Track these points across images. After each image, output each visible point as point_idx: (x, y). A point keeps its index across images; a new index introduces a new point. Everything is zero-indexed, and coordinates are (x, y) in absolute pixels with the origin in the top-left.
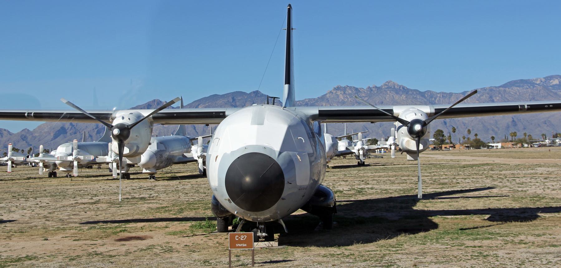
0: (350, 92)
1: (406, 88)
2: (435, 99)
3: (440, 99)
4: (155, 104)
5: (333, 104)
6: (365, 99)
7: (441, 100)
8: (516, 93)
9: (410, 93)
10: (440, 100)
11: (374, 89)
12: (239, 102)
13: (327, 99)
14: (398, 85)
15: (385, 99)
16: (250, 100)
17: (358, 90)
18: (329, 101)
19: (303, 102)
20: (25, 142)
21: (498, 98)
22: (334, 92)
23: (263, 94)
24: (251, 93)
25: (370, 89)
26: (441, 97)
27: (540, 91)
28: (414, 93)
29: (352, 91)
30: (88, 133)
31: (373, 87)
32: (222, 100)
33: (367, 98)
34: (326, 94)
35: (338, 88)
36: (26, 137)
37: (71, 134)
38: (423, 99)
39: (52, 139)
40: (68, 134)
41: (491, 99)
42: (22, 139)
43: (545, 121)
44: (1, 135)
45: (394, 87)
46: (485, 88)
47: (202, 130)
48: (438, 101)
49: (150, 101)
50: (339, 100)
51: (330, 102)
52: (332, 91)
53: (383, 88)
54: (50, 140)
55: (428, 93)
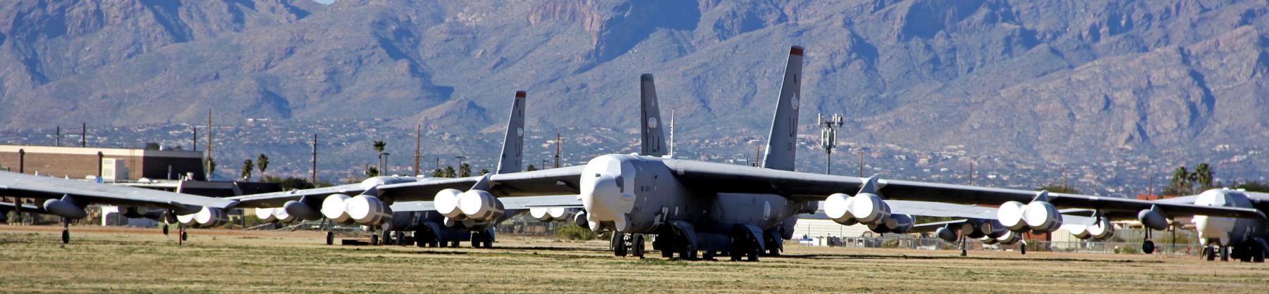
20: (403, 65)
30: (848, 23)
36: (409, 34)
37: (718, 26)
39: (588, 56)
40: (705, 27)
42: (385, 43)
44: (231, 10)
54: (578, 61)
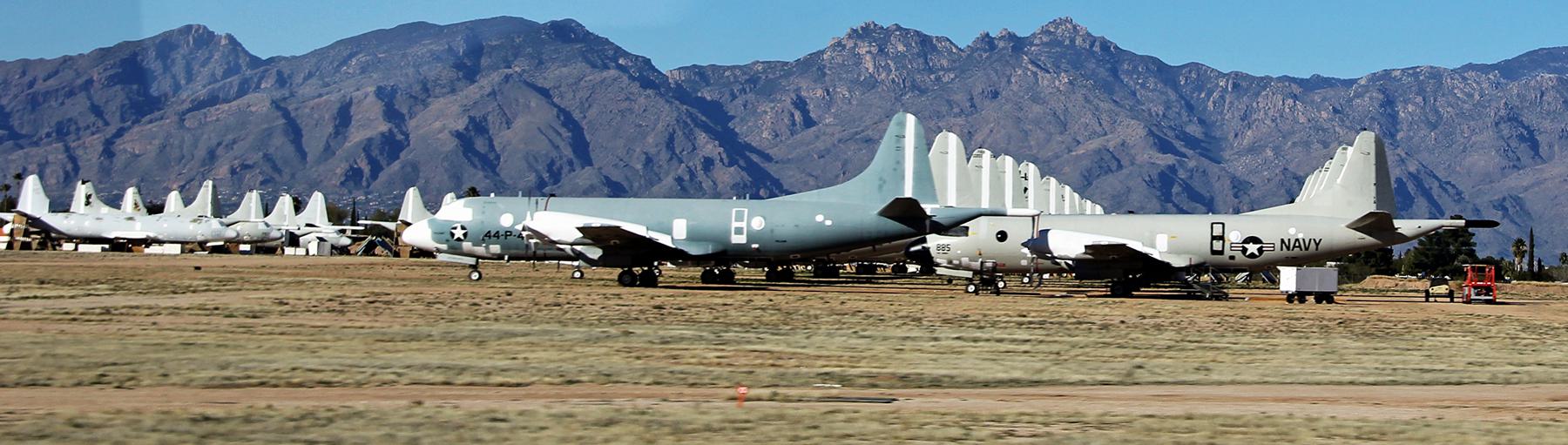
0: (901, 48)
1: (1116, 47)
2: (1209, 95)
3: (1222, 97)
4: (188, 42)
5: (835, 87)
6: (945, 79)
7: (1227, 102)
8: (1471, 96)
9: (1126, 66)
10: (1225, 102)
11: (1001, 44)
12: (490, 58)
13: (819, 69)
14: (1089, 35)
15: (1009, 82)
16: (529, 50)
17: (932, 41)
18: (824, 74)
19: (745, 74)
21: (1410, 108)
22: (850, 44)
25: (989, 42)
26: (1230, 89)
27: (1542, 95)
28: (1140, 69)
29: (907, 45)
31: (1002, 38)
32: (431, 44)
33: (952, 76)
34: (822, 52)
35: (866, 33)
38: (1162, 93)
41: (1389, 110)
43: (1504, 199)
45: (1073, 41)
46: (1418, 70)
47: (321, 146)
48: (1214, 103)
49: (173, 31)
50: (859, 75)
53: (1037, 41)
55: (1190, 72)
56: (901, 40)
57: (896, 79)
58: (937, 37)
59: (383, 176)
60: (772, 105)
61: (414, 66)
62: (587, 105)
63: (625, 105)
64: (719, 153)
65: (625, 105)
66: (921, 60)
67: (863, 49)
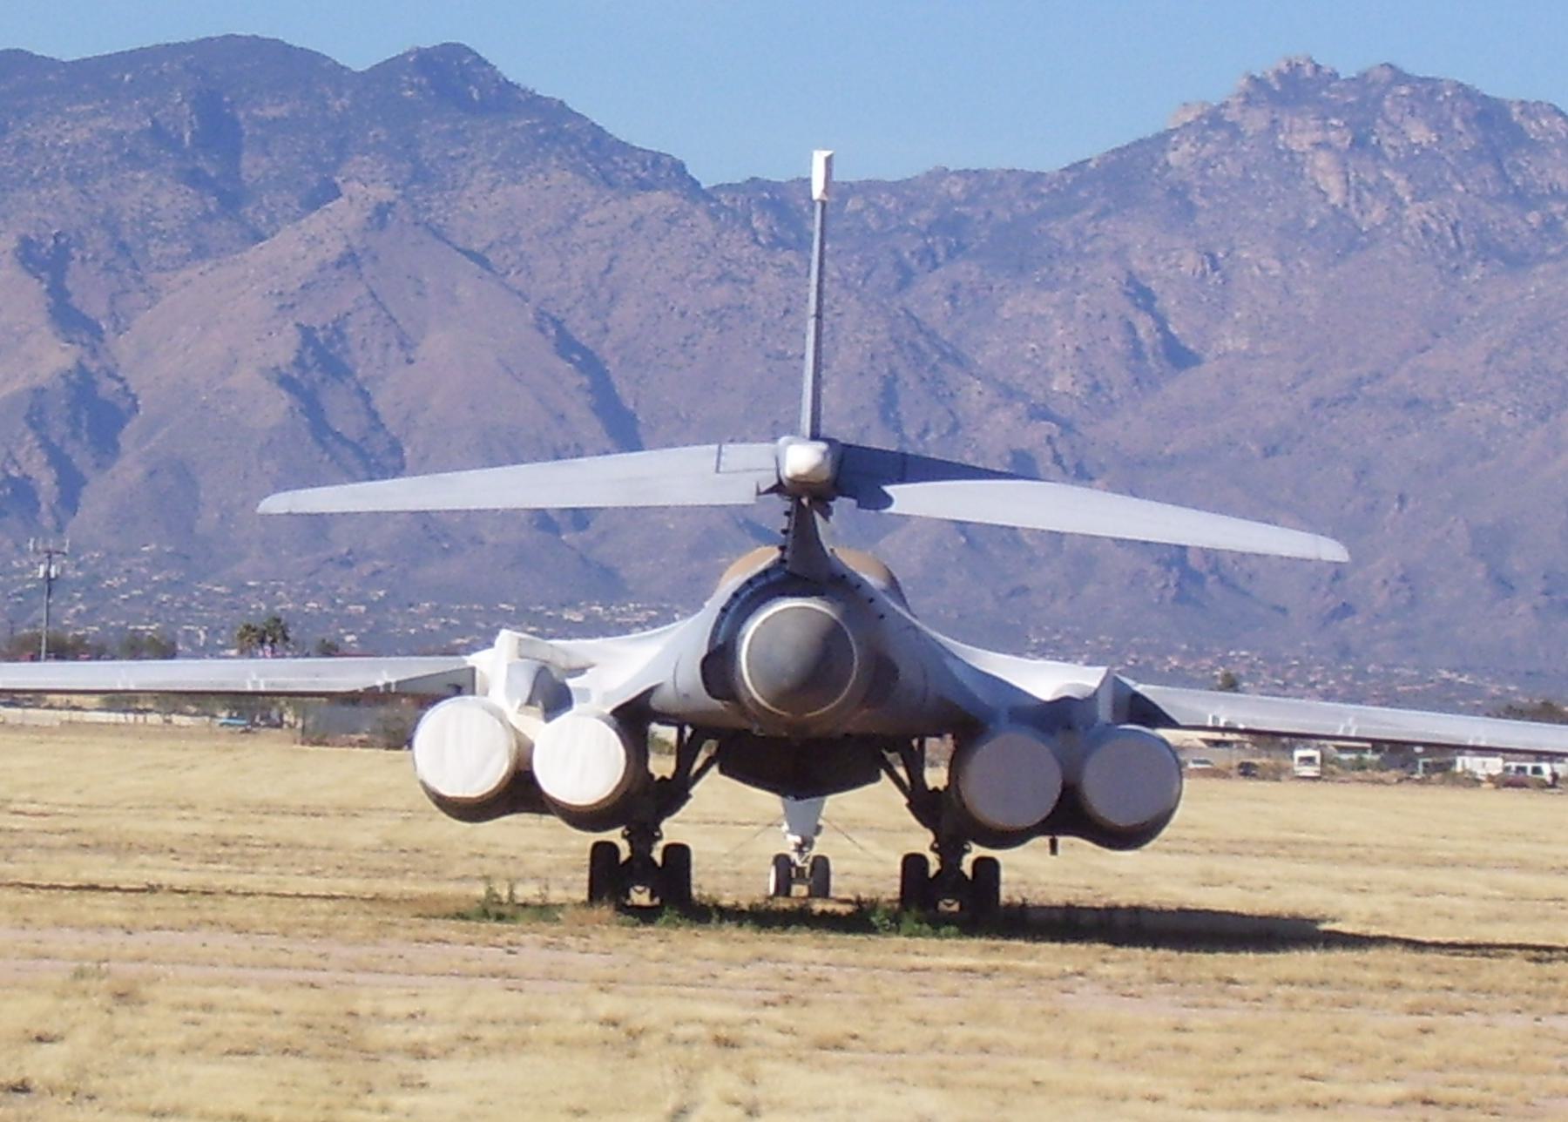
0: (1419, 133)
13: (1173, 192)
22: (1256, 121)
23: (510, 86)
24: (387, 71)
29: (1440, 126)
32: (96, 113)
34: (1162, 140)
51: (1202, 220)
52: (1232, 115)
56: (1418, 111)
57: (1434, 226)
58: (1522, 102)
59: (96, 502)
60: (1057, 296)
61: (71, 179)
62: (604, 295)
63: (722, 293)
64: (1049, 439)
65: (722, 293)
66: (1488, 171)
67: (1301, 135)
